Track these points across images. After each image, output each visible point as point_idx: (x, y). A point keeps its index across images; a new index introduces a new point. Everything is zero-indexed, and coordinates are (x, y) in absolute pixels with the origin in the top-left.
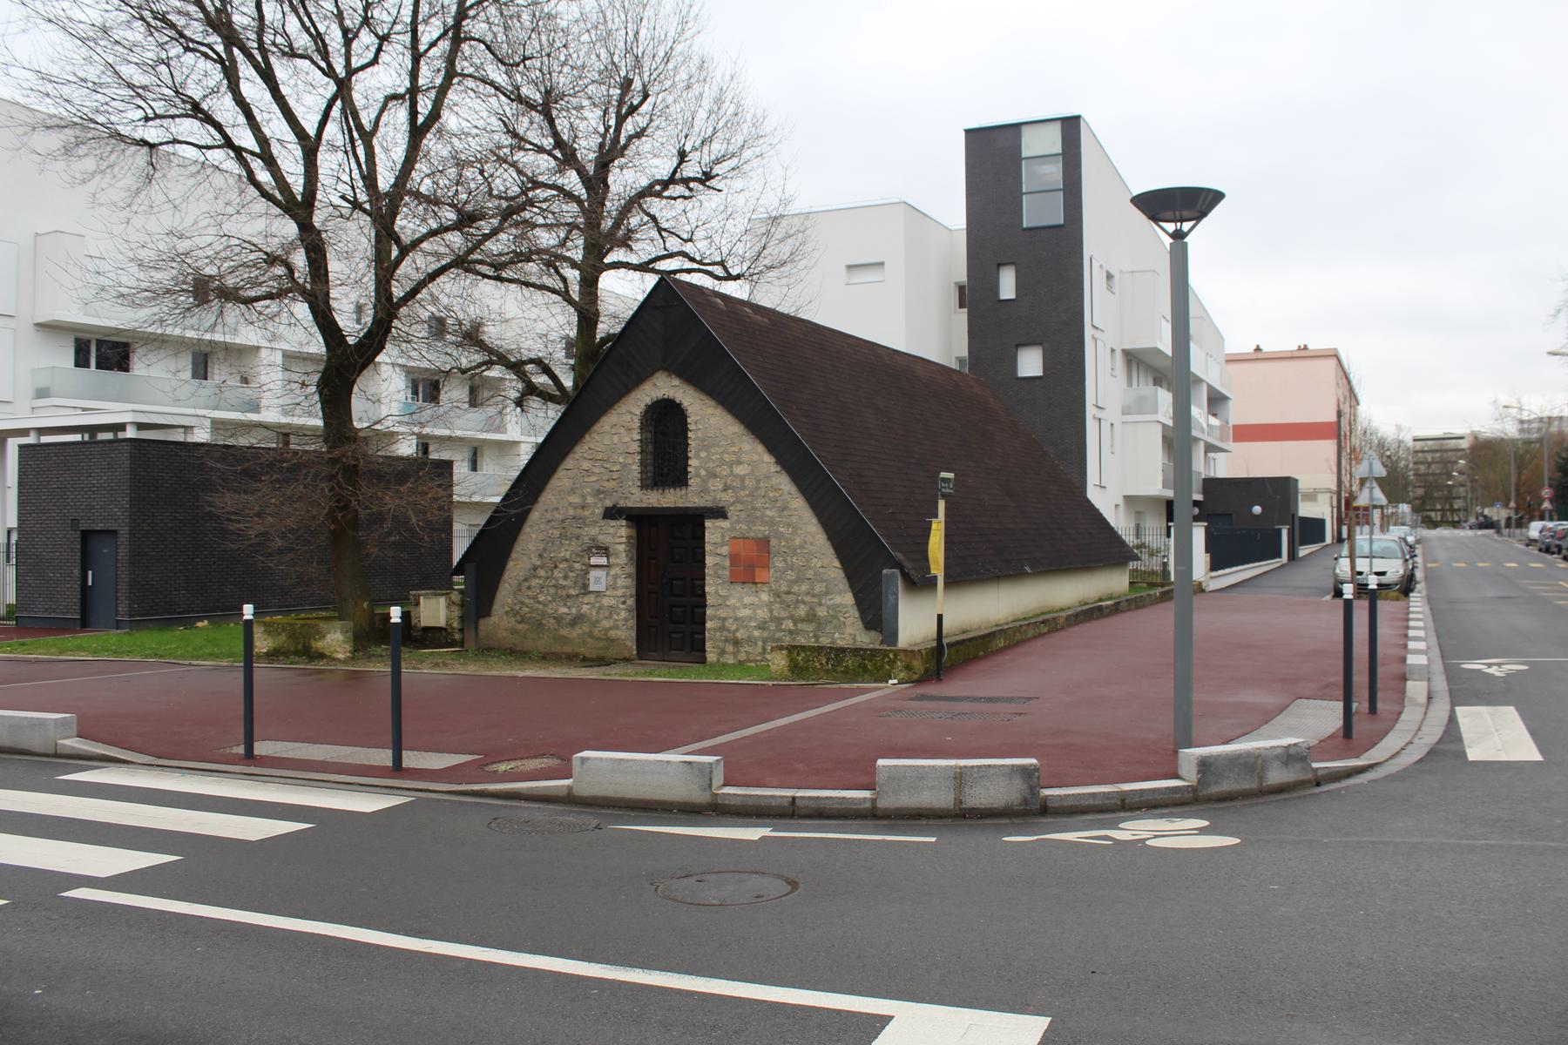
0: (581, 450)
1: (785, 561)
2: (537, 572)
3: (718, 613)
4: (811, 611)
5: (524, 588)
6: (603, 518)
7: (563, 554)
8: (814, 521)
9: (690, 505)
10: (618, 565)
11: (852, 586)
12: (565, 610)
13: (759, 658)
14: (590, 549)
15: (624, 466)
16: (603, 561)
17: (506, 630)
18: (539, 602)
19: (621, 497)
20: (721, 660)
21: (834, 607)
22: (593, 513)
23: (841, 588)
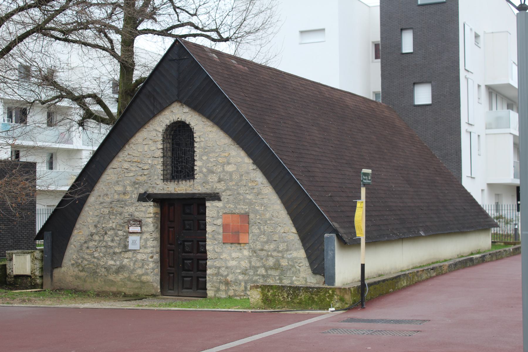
0: (122, 155)
1: (259, 229)
2: (94, 237)
3: (215, 263)
4: (277, 262)
5: (84, 248)
6: (138, 201)
7: (111, 225)
8: (279, 202)
9: (196, 192)
10: (147, 232)
11: (304, 245)
12: (112, 262)
13: (242, 294)
14: (129, 221)
15: (152, 166)
16: (138, 229)
17: (72, 276)
18: (94, 257)
19: (150, 187)
20: (217, 295)
21: (293, 259)
22: (131, 197)
23: (297, 246)
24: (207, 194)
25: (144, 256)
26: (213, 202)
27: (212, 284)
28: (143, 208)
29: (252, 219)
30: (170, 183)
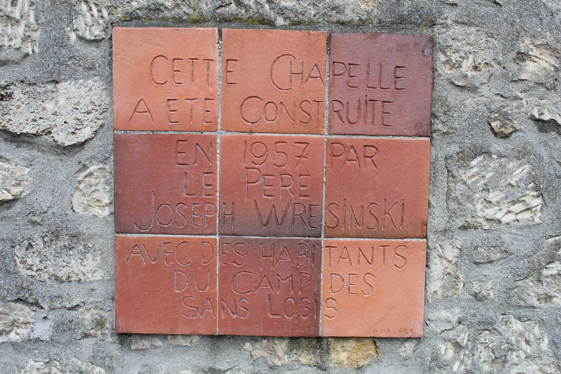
29: (472, 89)
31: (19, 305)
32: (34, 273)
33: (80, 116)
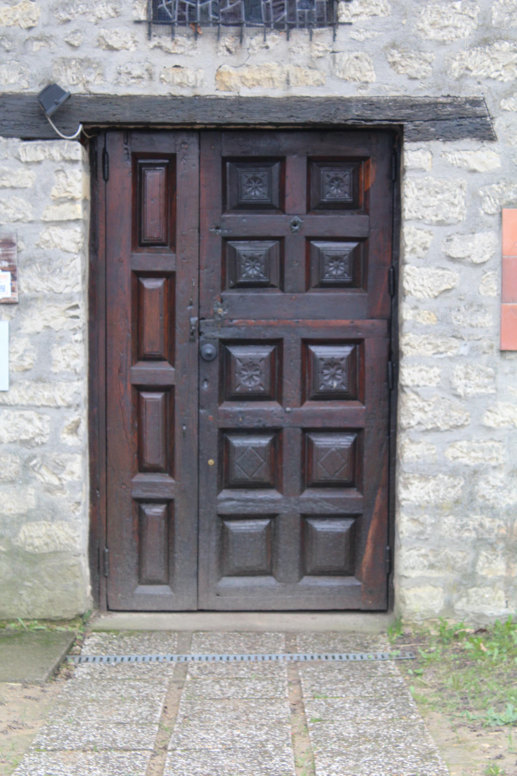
3: (450, 452)
19: (65, 62)
20: (459, 605)
24: (412, 107)
25: (30, 421)
26: (449, 146)
27: (436, 552)
28: (21, 170)
30: (189, 42)
31: (453, 339)
32: (460, 323)
33: (485, 249)
